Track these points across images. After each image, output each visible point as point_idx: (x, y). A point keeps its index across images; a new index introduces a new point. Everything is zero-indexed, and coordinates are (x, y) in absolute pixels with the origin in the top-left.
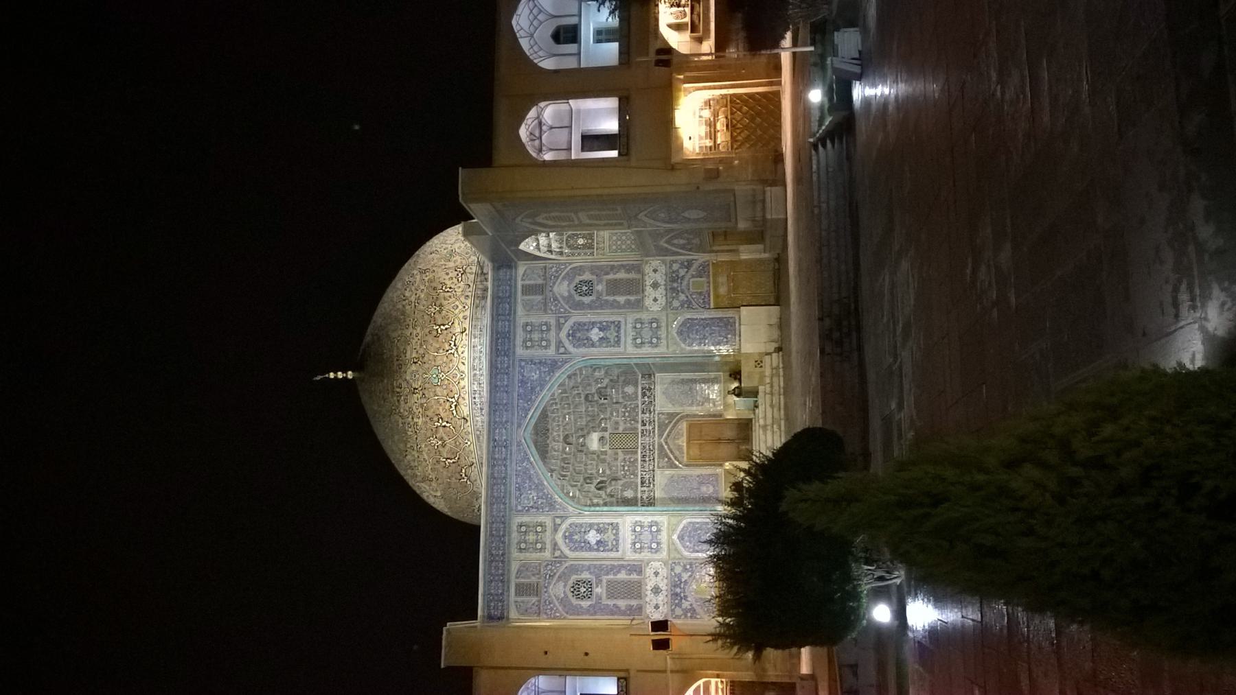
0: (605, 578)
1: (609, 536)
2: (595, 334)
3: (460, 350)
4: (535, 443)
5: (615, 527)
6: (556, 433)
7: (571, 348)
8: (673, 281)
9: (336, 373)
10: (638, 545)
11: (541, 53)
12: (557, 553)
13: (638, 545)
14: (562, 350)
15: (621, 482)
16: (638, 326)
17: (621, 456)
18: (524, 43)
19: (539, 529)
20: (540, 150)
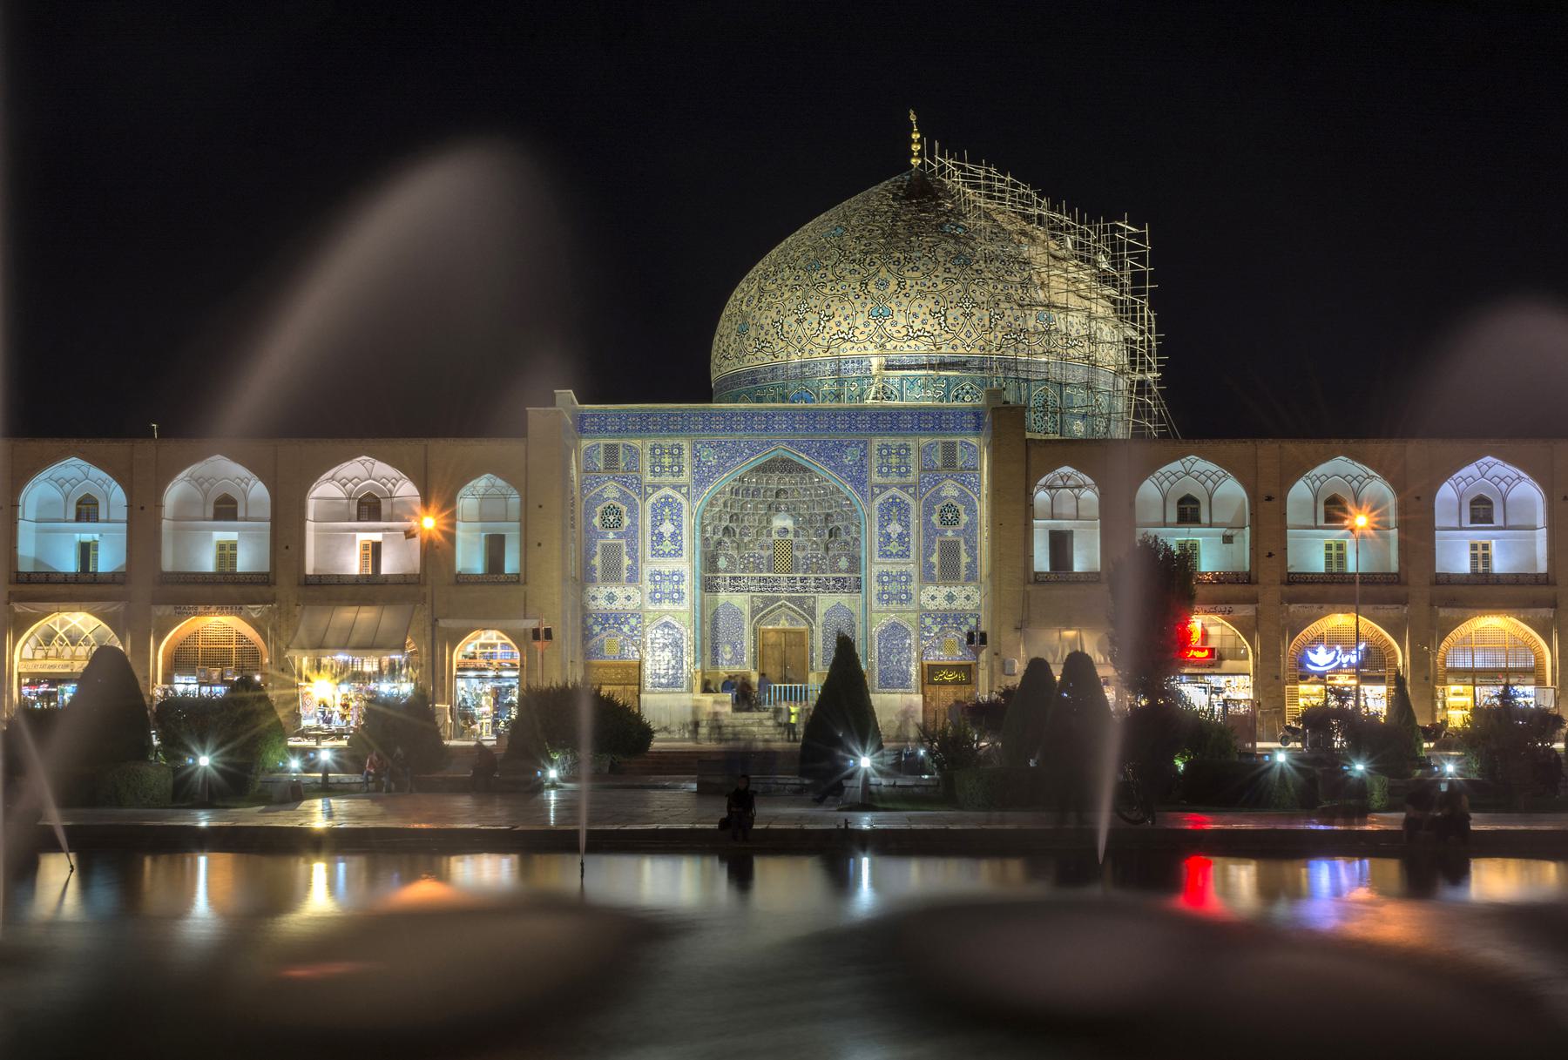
0: (623, 542)
1: (667, 546)
2: (895, 528)
3: (912, 343)
4: (773, 460)
5: (677, 553)
6: (788, 481)
7: (879, 500)
8: (955, 618)
9: (920, 141)
10: (658, 578)
11: (1166, 484)
12: (650, 490)
13: (658, 578)
14: (876, 490)
15: (735, 553)
16: (903, 578)
17: (766, 553)
18: (1176, 466)
19: (676, 469)
20: (1050, 487)
